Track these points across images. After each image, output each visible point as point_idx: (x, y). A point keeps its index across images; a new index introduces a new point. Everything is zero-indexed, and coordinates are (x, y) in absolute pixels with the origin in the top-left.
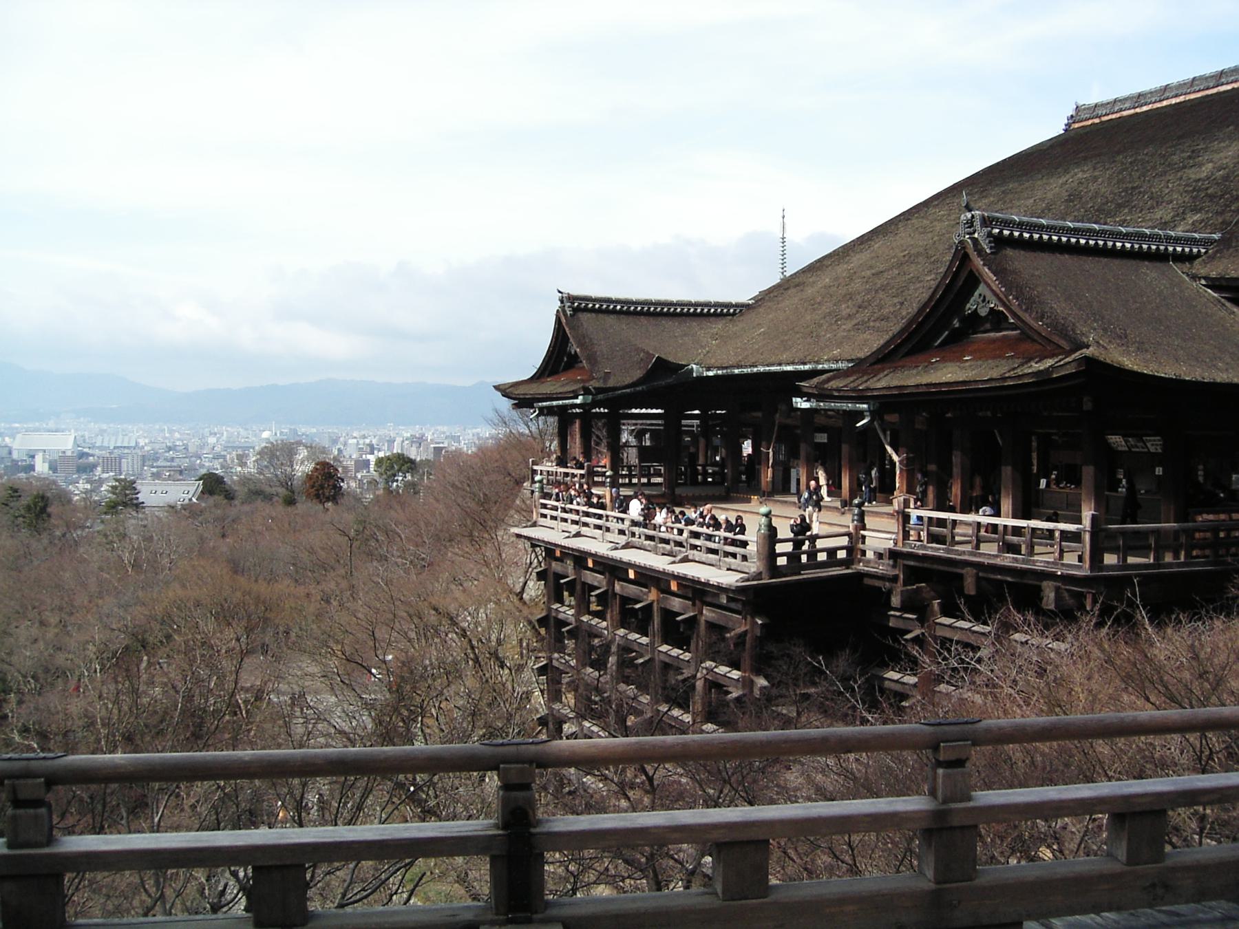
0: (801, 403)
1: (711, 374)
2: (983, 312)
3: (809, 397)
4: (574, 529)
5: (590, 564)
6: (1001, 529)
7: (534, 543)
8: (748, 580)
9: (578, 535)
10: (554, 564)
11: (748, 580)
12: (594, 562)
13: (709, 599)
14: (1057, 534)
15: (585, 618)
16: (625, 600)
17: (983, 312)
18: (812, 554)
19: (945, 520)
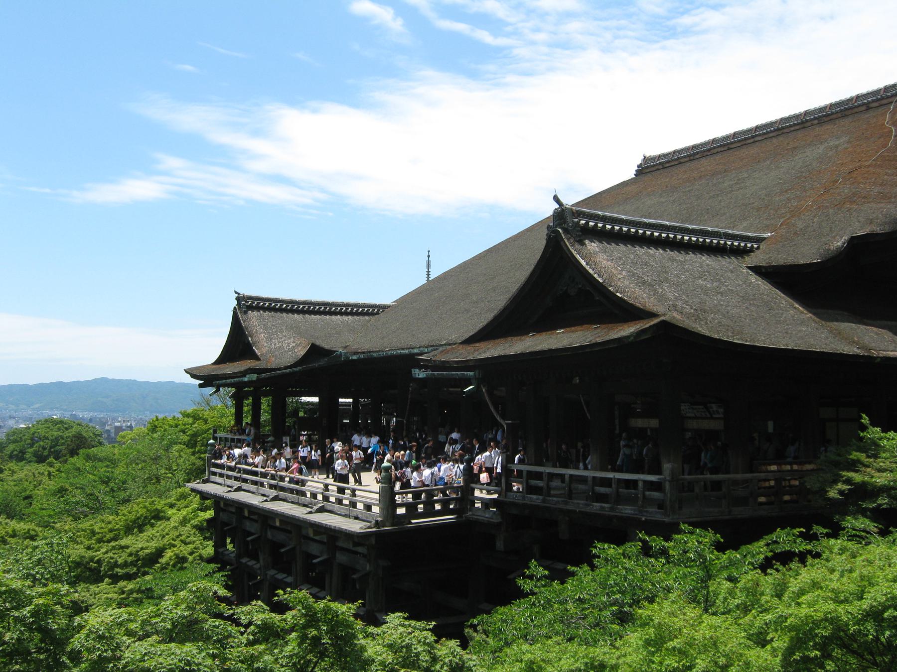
0: (420, 374)
1: (355, 357)
3: (426, 367)
4: (237, 484)
5: (246, 514)
6: (590, 479)
7: (204, 496)
8: (369, 527)
9: (239, 489)
10: (221, 514)
11: (369, 527)
12: (250, 512)
13: (340, 544)
14: (640, 484)
15: (244, 560)
16: (275, 546)
19: (541, 473)
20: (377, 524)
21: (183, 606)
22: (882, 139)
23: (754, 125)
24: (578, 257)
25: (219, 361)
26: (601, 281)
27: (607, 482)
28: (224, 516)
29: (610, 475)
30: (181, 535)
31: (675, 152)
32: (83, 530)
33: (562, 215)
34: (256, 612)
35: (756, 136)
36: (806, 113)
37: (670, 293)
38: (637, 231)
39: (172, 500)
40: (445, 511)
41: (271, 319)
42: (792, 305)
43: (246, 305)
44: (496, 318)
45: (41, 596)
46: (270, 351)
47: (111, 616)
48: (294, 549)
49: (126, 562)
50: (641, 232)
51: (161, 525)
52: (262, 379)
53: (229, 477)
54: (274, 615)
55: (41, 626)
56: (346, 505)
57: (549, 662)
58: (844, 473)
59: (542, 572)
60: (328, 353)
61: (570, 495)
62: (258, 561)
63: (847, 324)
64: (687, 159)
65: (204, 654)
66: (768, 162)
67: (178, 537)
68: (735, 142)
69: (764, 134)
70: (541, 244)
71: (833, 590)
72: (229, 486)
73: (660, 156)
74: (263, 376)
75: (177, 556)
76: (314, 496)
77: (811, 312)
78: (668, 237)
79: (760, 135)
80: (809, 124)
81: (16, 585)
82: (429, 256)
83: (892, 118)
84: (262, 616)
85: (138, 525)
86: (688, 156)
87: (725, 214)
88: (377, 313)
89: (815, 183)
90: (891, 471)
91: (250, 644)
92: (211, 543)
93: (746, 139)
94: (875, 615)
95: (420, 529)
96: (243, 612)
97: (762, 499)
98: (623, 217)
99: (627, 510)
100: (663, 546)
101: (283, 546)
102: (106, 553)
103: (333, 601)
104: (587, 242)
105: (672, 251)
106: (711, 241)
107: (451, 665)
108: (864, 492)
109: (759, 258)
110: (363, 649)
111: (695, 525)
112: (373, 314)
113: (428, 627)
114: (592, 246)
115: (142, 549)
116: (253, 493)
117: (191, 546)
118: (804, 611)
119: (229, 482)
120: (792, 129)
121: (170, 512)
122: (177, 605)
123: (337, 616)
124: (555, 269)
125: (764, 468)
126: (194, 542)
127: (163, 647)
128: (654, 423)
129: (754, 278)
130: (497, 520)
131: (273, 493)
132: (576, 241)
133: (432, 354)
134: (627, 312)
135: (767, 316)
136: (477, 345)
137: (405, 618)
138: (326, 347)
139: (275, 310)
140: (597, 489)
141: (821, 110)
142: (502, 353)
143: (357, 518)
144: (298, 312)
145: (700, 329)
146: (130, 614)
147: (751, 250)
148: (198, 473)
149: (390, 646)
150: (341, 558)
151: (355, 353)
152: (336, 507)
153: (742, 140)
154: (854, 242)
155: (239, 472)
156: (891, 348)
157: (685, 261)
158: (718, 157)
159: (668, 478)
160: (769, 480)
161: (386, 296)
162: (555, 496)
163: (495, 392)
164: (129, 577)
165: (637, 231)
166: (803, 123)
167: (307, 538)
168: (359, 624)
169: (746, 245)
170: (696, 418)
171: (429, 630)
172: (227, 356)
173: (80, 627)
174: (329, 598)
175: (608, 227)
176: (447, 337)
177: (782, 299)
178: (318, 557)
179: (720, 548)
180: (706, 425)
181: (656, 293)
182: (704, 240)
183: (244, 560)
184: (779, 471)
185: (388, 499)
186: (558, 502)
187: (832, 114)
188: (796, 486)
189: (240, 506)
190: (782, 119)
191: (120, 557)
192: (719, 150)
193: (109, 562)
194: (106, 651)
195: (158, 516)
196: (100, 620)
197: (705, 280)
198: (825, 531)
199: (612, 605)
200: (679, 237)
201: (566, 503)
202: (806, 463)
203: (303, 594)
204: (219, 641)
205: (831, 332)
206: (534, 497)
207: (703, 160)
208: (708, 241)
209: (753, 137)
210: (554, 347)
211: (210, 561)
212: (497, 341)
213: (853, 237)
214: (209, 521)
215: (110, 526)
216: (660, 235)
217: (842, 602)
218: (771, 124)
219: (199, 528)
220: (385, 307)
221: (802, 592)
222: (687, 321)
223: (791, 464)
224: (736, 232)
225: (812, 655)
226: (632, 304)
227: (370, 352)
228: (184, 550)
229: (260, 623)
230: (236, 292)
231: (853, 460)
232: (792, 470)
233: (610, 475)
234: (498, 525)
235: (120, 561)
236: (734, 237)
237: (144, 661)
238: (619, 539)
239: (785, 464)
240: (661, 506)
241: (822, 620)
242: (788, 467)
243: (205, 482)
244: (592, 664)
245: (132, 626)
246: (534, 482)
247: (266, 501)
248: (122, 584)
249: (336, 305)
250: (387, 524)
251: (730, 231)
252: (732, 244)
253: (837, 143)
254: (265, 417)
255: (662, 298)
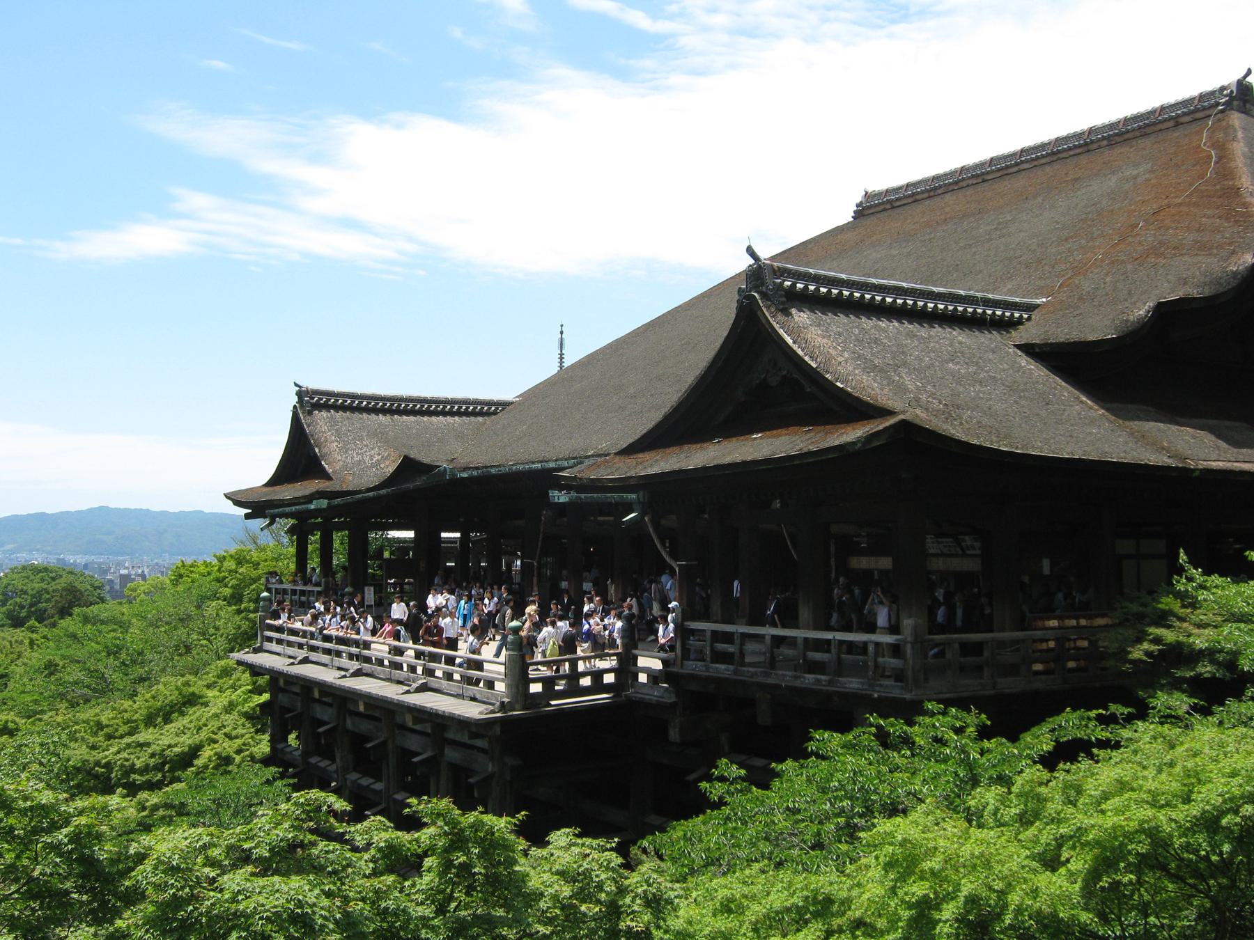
1: (465, 475)
2: (774, 381)
3: (568, 488)
4: (301, 654)
5: (316, 695)
7: (255, 671)
8: (492, 712)
9: (306, 661)
10: (280, 696)
11: (492, 712)
13: (450, 735)
14: (871, 648)
15: (314, 760)
16: (358, 740)
17: (774, 381)
18: (575, 676)
19: (732, 634)
20: (503, 707)
21: (286, 825)
22: (1198, 167)
23: (1019, 148)
24: (781, 332)
25: (273, 482)
26: (814, 365)
27: (823, 645)
28: (283, 699)
29: (829, 635)
30: (224, 726)
31: (908, 185)
32: (84, 722)
33: (758, 274)
34: (377, 831)
35: (1022, 162)
36: (1091, 131)
37: (909, 382)
38: (862, 296)
39: (211, 678)
40: (598, 686)
41: (346, 422)
42: (1077, 398)
43: (311, 402)
44: (667, 418)
45: (81, 813)
46: (345, 467)
47: (186, 839)
48: (384, 743)
49: (147, 765)
50: (868, 297)
51: (194, 713)
52: (335, 507)
53: (290, 644)
54: (400, 834)
55: (84, 854)
56: (457, 681)
57: (753, 898)
58: (1152, 630)
59: (735, 771)
60: (428, 468)
61: (772, 663)
62: (333, 760)
63: (1152, 424)
64: (926, 195)
65: (317, 891)
66: (1040, 199)
67: (219, 729)
68: (993, 171)
69: (1033, 160)
70: (727, 315)
71: (1149, 791)
72: (290, 657)
73: (887, 191)
74: (337, 502)
75: (219, 755)
76: (413, 669)
77: (1103, 408)
78: (905, 303)
79: (1026, 161)
80: (1095, 146)
81: (47, 797)
82: (562, 333)
83: (1210, 137)
84: (385, 835)
85: (166, 714)
86: (927, 191)
87: (981, 271)
88: (495, 413)
89: (1106, 229)
90: (1216, 627)
91: (376, 873)
92: (267, 737)
93: (1007, 167)
94: (1209, 823)
95: (562, 712)
96: (357, 832)
97: (1038, 667)
98: (843, 276)
99: (853, 684)
100: (905, 733)
101: (368, 739)
102: (118, 752)
103: (486, 812)
104: (794, 311)
105: (911, 323)
106: (965, 310)
107: (646, 897)
108: (1180, 655)
109: (1030, 333)
110: (524, 877)
111: (948, 703)
112: (488, 414)
113: (609, 846)
114: (801, 317)
115: (170, 746)
116: (325, 665)
117: (238, 742)
118: (1110, 821)
119: (291, 651)
120: (1072, 153)
121: (211, 693)
122: (278, 824)
123: (493, 833)
124: (748, 352)
125: (1040, 623)
126: (243, 736)
127: (261, 882)
128: (885, 563)
129: (1024, 361)
130: (671, 699)
131: (354, 665)
132: (778, 310)
133: (577, 469)
134: (852, 408)
135: (1043, 413)
136: (640, 456)
137: (575, 835)
138: (425, 460)
139: (352, 409)
140: (813, 655)
141: (1112, 126)
142: (676, 467)
143: (473, 699)
144: (384, 411)
145: (953, 432)
146: (212, 835)
147: (1020, 322)
148: (247, 638)
149: (562, 874)
150: (451, 755)
151: (465, 469)
152: (444, 684)
153: (1002, 169)
154: (1163, 310)
155: (304, 636)
156: (1214, 456)
157: (930, 336)
158: (970, 191)
159: (909, 639)
160: (1047, 641)
161: (507, 389)
162: (751, 665)
163: (663, 522)
164: (152, 786)
165: (862, 296)
166: (1086, 144)
167: (403, 727)
168: (522, 843)
169: (1012, 315)
170: (942, 555)
171: (612, 849)
172: (284, 475)
173: (141, 858)
174: (480, 809)
175: (823, 290)
176: (598, 444)
177: (1063, 390)
178: (418, 754)
179: (984, 733)
180: (957, 564)
181: (891, 382)
182: (955, 309)
183: (314, 760)
184: (1060, 628)
185: (519, 673)
186: (756, 673)
187: (1128, 131)
188: (1084, 649)
189: (307, 685)
190: (1057, 140)
191: (138, 758)
192: (970, 182)
193: (122, 766)
194: (183, 888)
195: (192, 700)
196: (172, 845)
197: (958, 363)
198: (1126, 710)
199: (838, 815)
200: (921, 304)
201: (766, 675)
202: (1097, 616)
203: (444, 803)
204: (335, 872)
205: (1132, 434)
206: (723, 667)
207: (948, 197)
208: (960, 309)
209: (1017, 164)
210: (749, 458)
211: (267, 761)
212: (668, 451)
213: (1160, 303)
214: (263, 706)
215: (126, 715)
216: (895, 301)
217: (1162, 807)
218: (1042, 146)
219: (248, 716)
220: (505, 404)
221: (1106, 797)
222: (934, 420)
223: (1077, 618)
224: (999, 297)
225: (1126, 880)
226: (857, 398)
227: (486, 467)
228: (228, 747)
229: (382, 844)
230: (296, 385)
231: (1163, 610)
232: (1078, 627)
233: (829, 635)
234: (673, 705)
235: (138, 764)
236: (996, 304)
237: (238, 902)
238: (842, 724)
239: (1070, 618)
240: (899, 676)
241: (1137, 831)
242: (1073, 622)
243: (256, 651)
244: (815, 898)
245: (215, 853)
246: (721, 647)
247: (344, 677)
248: (144, 795)
249: (437, 401)
250: (517, 706)
251: (990, 296)
252: (994, 313)
253: (1135, 172)
254: (338, 560)
255: (900, 389)
